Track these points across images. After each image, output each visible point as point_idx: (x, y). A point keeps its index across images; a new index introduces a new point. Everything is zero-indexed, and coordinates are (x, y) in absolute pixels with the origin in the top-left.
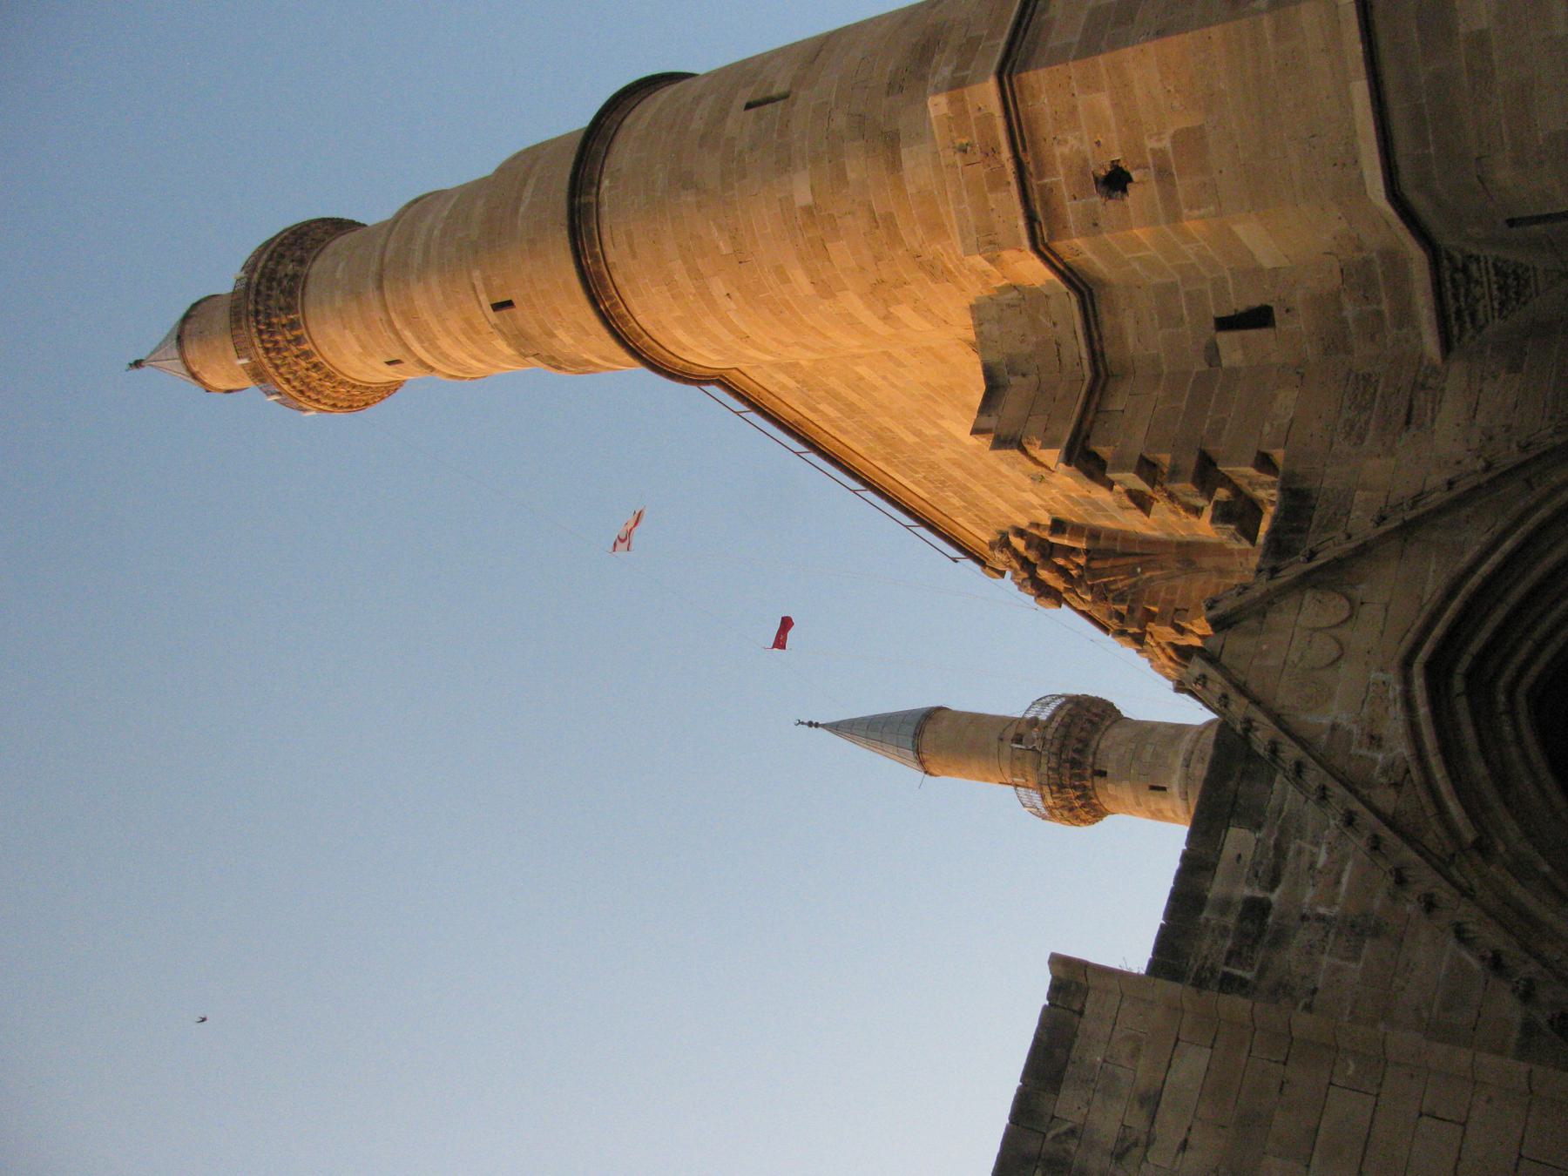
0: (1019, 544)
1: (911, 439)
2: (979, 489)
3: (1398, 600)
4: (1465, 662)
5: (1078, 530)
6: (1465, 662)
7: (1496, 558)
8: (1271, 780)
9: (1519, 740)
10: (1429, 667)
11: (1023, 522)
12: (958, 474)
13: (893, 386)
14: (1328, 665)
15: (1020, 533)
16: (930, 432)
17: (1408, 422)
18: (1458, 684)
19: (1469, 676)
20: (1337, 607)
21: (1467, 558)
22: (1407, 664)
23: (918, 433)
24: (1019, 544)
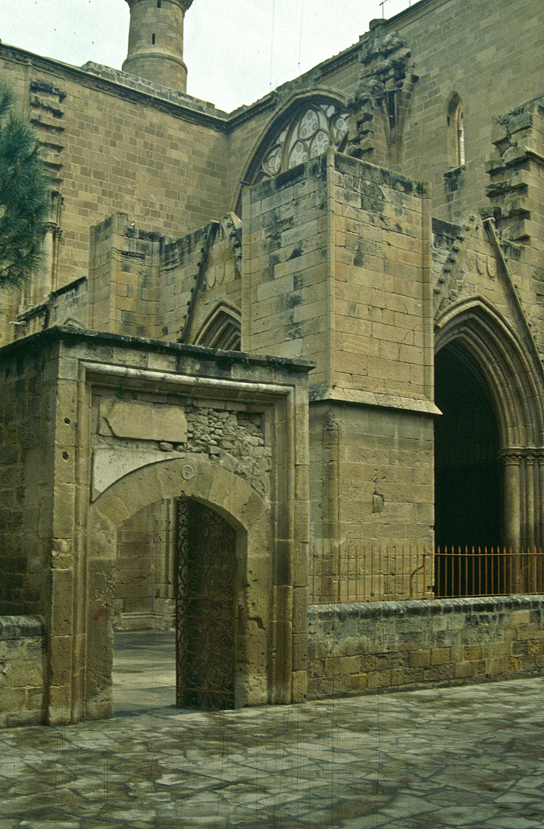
0: (403, 52)
1: (483, 24)
2: (442, 46)
3: (494, 294)
4: (477, 318)
5: (412, 88)
6: (477, 318)
7: (506, 329)
8: (448, 249)
9: (453, 335)
10: (478, 307)
11: (416, 59)
12: (455, 39)
13: (522, 34)
14: (478, 269)
15: (408, 55)
16: (487, 38)
17: (538, 295)
18: (471, 316)
19: (472, 320)
20: (493, 271)
21: (506, 319)
22: (479, 298)
23: (486, 30)
24: (403, 52)
